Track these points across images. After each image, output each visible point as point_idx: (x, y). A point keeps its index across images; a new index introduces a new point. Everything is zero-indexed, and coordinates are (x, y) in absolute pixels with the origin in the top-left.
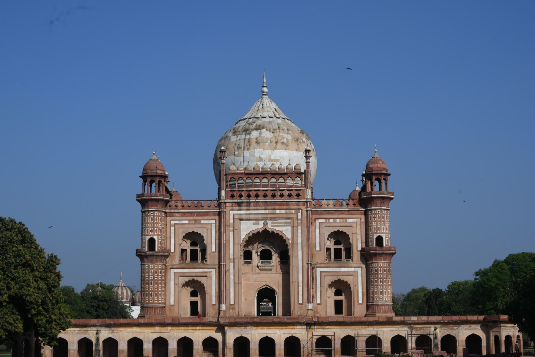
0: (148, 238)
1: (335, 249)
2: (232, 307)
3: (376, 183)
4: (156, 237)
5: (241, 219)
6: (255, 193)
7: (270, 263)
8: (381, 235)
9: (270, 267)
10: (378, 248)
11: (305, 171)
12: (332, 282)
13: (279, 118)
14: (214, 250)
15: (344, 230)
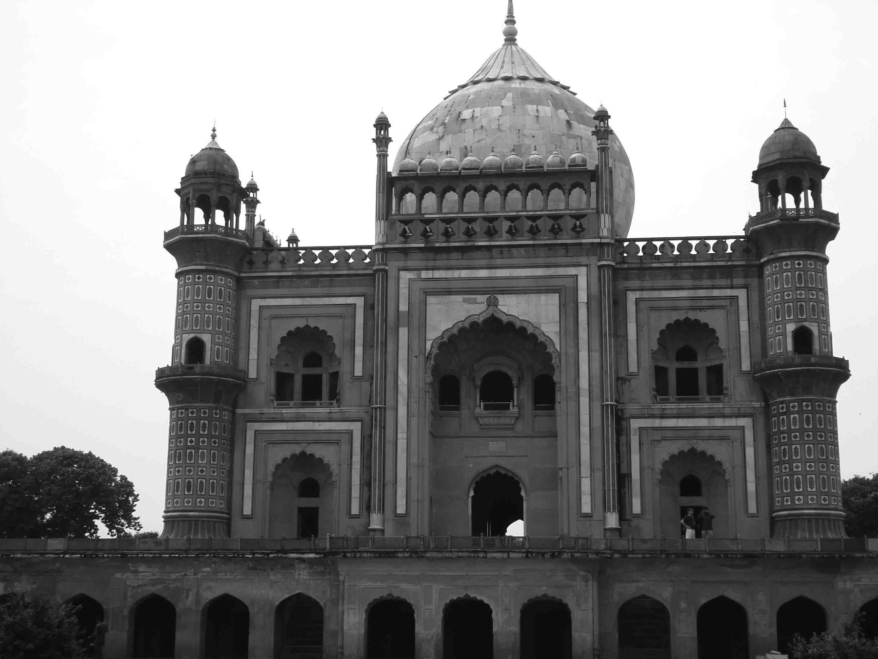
0: (187, 337)
1: (678, 371)
2: (401, 520)
3: (790, 199)
4: (206, 338)
5: (427, 293)
6: (464, 226)
7: (507, 407)
8: (806, 324)
9: (507, 421)
10: (798, 359)
11: (597, 166)
12: (673, 457)
13: (541, 80)
14: (358, 372)
15: (703, 317)
